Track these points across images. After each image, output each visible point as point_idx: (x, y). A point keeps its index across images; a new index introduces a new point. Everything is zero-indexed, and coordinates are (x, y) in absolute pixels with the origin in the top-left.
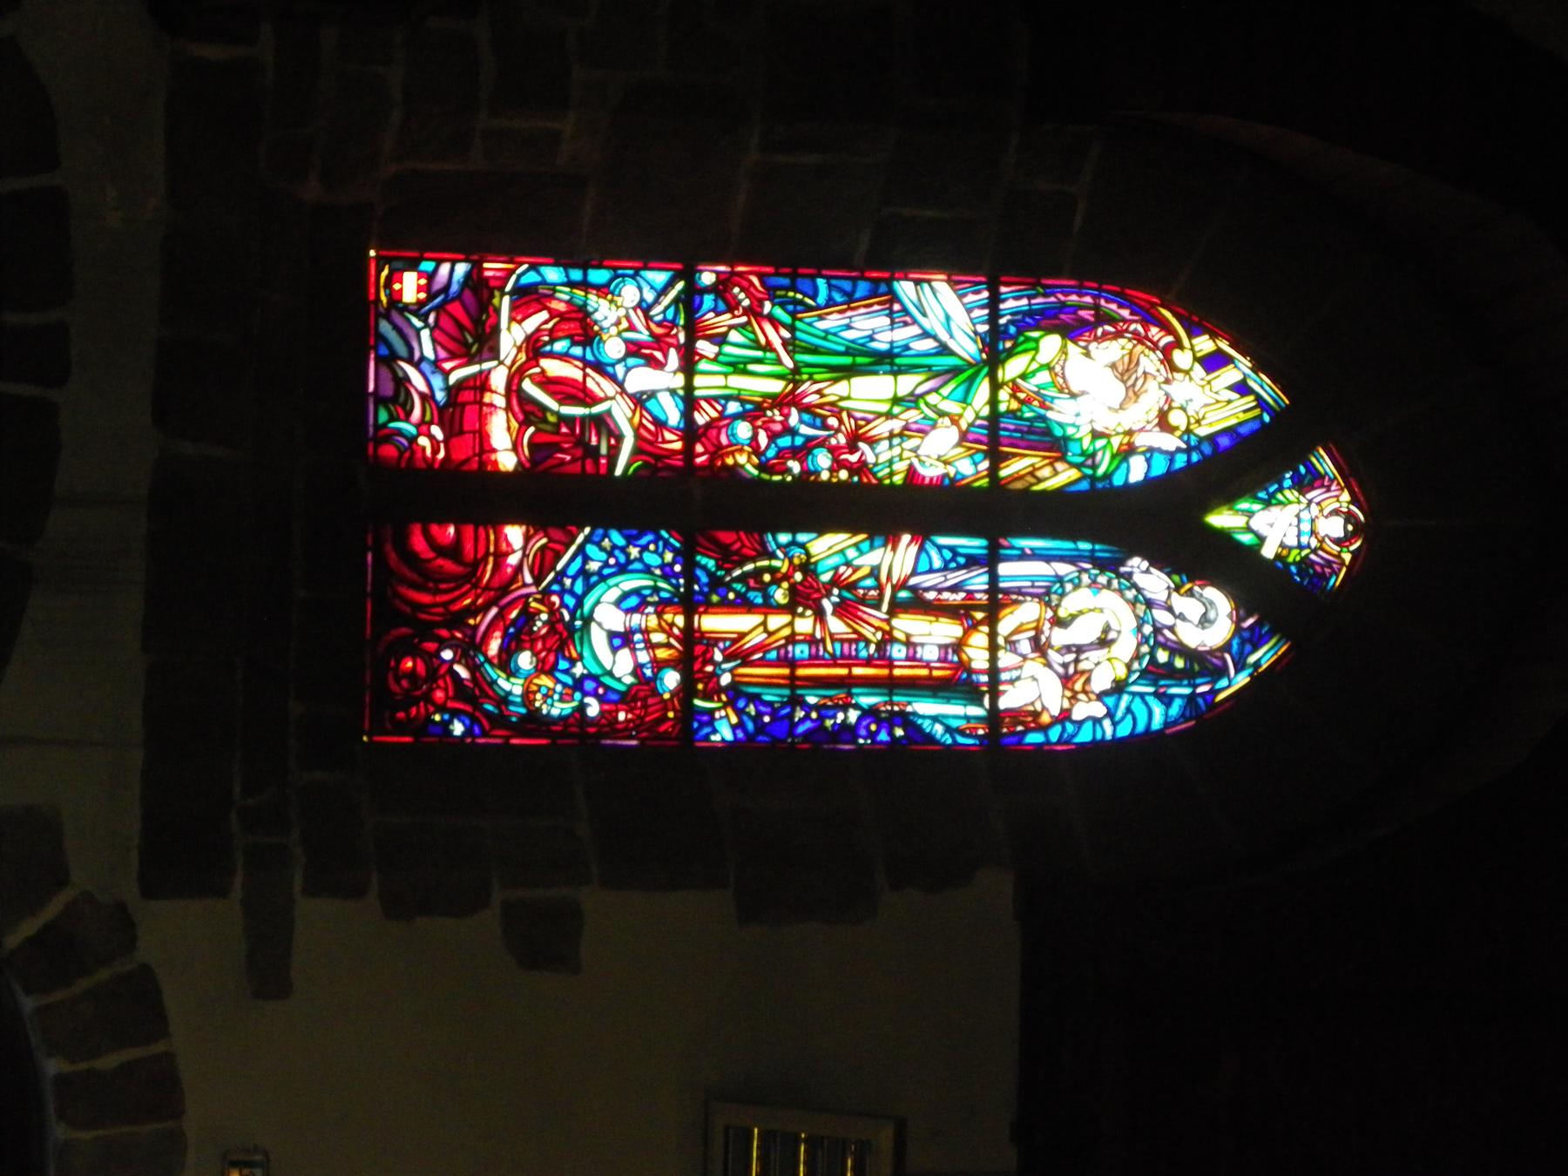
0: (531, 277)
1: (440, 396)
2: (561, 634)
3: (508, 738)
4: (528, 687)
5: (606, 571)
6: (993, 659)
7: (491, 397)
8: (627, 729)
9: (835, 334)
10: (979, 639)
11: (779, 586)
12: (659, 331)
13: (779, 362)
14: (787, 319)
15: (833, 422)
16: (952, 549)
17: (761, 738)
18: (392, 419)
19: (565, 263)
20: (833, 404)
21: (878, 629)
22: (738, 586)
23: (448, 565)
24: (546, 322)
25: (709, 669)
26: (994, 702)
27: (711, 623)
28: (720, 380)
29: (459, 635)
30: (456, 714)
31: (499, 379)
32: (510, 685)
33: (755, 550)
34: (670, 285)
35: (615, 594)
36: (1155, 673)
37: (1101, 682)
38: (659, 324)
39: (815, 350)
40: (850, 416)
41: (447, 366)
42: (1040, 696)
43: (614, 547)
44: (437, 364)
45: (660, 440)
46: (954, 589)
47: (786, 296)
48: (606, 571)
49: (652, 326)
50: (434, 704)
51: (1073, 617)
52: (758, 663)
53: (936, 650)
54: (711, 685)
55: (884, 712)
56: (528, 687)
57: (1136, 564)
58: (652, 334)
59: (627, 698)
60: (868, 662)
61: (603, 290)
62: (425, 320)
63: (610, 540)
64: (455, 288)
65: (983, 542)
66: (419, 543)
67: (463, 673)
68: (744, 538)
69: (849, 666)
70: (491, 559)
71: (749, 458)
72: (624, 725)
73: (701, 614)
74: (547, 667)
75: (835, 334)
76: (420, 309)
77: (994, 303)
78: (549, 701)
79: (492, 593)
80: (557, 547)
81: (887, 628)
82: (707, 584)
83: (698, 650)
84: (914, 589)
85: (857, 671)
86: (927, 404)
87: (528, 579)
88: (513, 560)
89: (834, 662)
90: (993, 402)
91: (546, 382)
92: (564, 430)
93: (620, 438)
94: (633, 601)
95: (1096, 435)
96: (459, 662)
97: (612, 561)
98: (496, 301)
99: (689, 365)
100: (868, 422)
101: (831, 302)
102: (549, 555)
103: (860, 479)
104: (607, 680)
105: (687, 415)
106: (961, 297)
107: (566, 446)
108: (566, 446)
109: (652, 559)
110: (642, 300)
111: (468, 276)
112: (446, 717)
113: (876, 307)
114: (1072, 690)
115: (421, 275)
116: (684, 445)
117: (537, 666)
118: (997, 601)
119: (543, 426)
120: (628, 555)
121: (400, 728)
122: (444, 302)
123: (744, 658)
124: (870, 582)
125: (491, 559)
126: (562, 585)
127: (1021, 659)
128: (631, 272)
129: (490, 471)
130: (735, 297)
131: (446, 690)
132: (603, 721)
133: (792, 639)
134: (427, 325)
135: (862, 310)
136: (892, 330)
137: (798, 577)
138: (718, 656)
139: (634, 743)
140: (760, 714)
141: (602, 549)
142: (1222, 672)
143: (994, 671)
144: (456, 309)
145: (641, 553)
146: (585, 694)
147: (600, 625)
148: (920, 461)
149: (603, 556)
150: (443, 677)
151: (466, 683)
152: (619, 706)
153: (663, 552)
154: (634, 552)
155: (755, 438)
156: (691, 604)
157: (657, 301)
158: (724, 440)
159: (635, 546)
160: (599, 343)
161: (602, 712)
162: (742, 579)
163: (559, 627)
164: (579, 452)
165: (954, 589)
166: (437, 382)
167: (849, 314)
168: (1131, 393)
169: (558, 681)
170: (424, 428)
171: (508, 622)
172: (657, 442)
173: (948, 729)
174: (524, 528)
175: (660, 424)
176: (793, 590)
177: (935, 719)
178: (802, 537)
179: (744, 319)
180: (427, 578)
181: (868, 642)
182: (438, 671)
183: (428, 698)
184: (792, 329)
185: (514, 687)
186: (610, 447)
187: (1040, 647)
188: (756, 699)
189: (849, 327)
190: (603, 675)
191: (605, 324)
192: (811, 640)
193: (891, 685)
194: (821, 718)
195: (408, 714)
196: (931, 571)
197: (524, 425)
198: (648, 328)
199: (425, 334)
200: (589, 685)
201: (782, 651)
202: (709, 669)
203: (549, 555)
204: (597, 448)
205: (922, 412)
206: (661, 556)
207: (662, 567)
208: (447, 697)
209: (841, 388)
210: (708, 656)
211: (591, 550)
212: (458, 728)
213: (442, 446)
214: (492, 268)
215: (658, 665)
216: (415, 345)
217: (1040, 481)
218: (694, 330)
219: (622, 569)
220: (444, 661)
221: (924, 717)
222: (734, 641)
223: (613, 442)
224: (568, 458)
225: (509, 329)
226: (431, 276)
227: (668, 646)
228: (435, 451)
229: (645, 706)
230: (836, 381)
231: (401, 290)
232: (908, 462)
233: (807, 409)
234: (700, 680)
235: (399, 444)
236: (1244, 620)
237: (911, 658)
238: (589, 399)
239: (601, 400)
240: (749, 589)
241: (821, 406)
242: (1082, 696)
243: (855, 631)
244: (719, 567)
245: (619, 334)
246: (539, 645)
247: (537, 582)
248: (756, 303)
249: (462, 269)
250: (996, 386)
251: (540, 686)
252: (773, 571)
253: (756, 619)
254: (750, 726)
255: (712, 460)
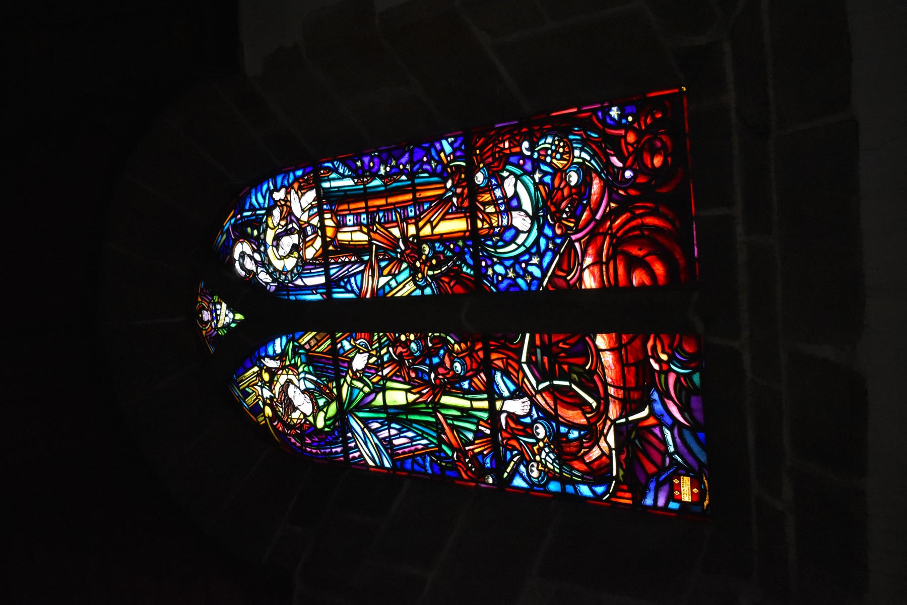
0: (600, 490)
1: (655, 396)
2: (552, 203)
3: (579, 112)
4: (569, 157)
5: (526, 257)
6: (322, 220)
7: (618, 394)
8: (504, 135)
9: (418, 435)
10: (330, 232)
11: (427, 256)
12: (514, 443)
13: (444, 415)
14: (444, 447)
15: (413, 375)
16: (348, 291)
17: (427, 145)
18: (688, 377)
19: (578, 496)
20: (414, 387)
21: (375, 232)
22: (449, 254)
23: (636, 252)
24: (586, 453)
25: (459, 190)
26: (318, 193)
27: (459, 225)
28: (476, 404)
29: (621, 192)
30: (617, 124)
31: (613, 411)
32: (582, 156)
33: (443, 282)
34: (512, 476)
35: (521, 239)
36: (258, 223)
37: (276, 212)
38: (515, 448)
39: (427, 424)
40: (404, 378)
41: (652, 421)
42: (300, 199)
43: (523, 277)
44: (661, 424)
45: (505, 360)
46: (344, 264)
47: (446, 463)
48: (526, 257)
49: (518, 446)
50: (635, 131)
51: (291, 252)
52: (433, 199)
53: (349, 223)
54: (457, 178)
55: (368, 176)
56: (569, 157)
57: (272, 287)
58: (518, 440)
59: (505, 159)
60: (379, 208)
61: (550, 476)
62: (673, 460)
63: (526, 281)
64: (652, 486)
65: (336, 296)
66: (659, 269)
67: (615, 160)
68: (449, 290)
69: (387, 204)
70: (604, 260)
71: (453, 348)
72: (504, 138)
73: (467, 230)
74: (559, 174)
75: (418, 435)
76: (677, 470)
77: (346, 450)
78: (554, 148)
79: (601, 231)
80: (560, 273)
81: (372, 234)
82: (466, 253)
83: (466, 204)
84: (362, 262)
85: (382, 202)
86: (369, 387)
87: (577, 245)
88: (588, 261)
89: (395, 207)
90: (339, 388)
91: (581, 405)
92: (565, 367)
93: (528, 362)
94: (508, 235)
95: (295, 366)
96: (619, 168)
97: (523, 265)
98: (621, 473)
99: (494, 414)
100: (395, 374)
101: (423, 456)
102: (565, 267)
103: (395, 335)
104: (518, 172)
105: (491, 381)
106: (361, 456)
107: (563, 354)
108: (563, 354)
109: (499, 269)
110: (526, 467)
111: (644, 496)
112: (624, 121)
113: (400, 452)
114: (287, 206)
115: (679, 500)
116: (490, 357)
117: (566, 174)
118: (323, 260)
119: (581, 370)
120: (514, 271)
121: (658, 103)
122: (659, 474)
123: (442, 201)
124: (383, 264)
125: (604, 260)
126: (554, 243)
127: (311, 222)
128: (535, 488)
129: (613, 332)
130: (474, 465)
131: (627, 143)
132: (518, 138)
133: (417, 219)
134: (671, 455)
135: (407, 450)
136: (390, 436)
137: (418, 264)
138: (455, 200)
139: (497, 126)
140: (428, 163)
141: (531, 274)
142: (234, 226)
143: (321, 214)
144: (651, 469)
145: (507, 273)
146: (530, 158)
147: (527, 214)
148: (367, 348)
149: (530, 269)
150: (630, 154)
151: (612, 153)
152: (508, 152)
153: (493, 275)
154: (511, 275)
155: (452, 363)
156: (473, 236)
157: (518, 464)
158: (467, 359)
159: (510, 278)
160: (550, 434)
161: (520, 146)
162: (448, 259)
163: (553, 209)
164: (554, 349)
165: (344, 264)
166: (658, 407)
167: (413, 448)
168: (285, 390)
169: (550, 165)
170: (665, 367)
171: (588, 208)
172: (507, 359)
173: (336, 170)
174: (583, 287)
175: (506, 373)
176: (420, 252)
177: (343, 176)
178: (418, 292)
179: (467, 448)
180: (647, 237)
181: (380, 223)
182: (635, 159)
183: (639, 133)
184: (441, 441)
185: (581, 155)
186: (536, 355)
187: (302, 232)
188: (433, 173)
189: (412, 439)
190: (522, 175)
191: (547, 450)
192: (406, 219)
193: (366, 195)
194: (397, 166)
195: (653, 117)
196: (355, 275)
197: (592, 372)
198: (521, 445)
199: (672, 449)
200: (528, 167)
201: (421, 210)
202: (459, 190)
203: (565, 267)
204: (542, 355)
205: (370, 380)
206: (494, 272)
207: (494, 264)
208: (625, 137)
209: (412, 397)
210: (460, 200)
211: (537, 272)
212: (614, 112)
213: (650, 354)
214: (626, 500)
215: (489, 189)
216: (678, 440)
217: (314, 337)
218: (492, 441)
219: (517, 259)
220: (630, 168)
221: (348, 176)
222: (447, 213)
223: (534, 358)
224: (561, 345)
225: (610, 449)
226: (671, 497)
227: (485, 204)
228: (654, 348)
229: (493, 155)
230: (415, 402)
231: (692, 488)
232: (374, 347)
233: (428, 383)
234: (464, 180)
235: (682, 354)
236: (230, 258)
237: (358, 215)
238: (552, 390)
239: (544, 389)
240: (442, 252)
241: (420, 385)
242: (283, 203)
243: (386, 229)
244: (460, 267)
245: (538, 440)
246: (566, 192)
247: (572, 243)
248: (462, 459)
249: (649, 501)
250: (339, 398)
251: (562, 159)
252: (432, 268)
253: (439, 230)
254: (433, 153)
255: (473, 346)
